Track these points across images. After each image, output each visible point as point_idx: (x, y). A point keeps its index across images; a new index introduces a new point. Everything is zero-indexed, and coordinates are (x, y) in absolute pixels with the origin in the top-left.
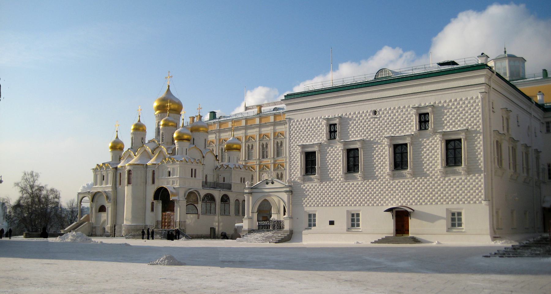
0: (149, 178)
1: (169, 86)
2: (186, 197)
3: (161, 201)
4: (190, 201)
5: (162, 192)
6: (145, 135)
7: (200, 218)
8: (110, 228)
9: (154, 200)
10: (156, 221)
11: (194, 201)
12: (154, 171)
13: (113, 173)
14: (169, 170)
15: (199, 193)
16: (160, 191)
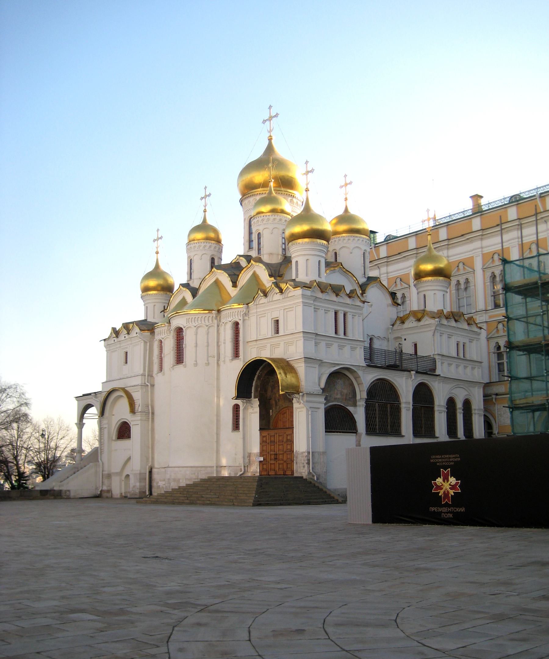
0: (225, 343)
1: (270, 140)
2: (323, 385)
3: (256, 402)
4: (335, 399)
5: (259, 378)
6: (220, 251)
7: (361, 443)
8: (138, 477)
9: (238, 397)
10: (247, 455)
11: (346, 399)
12: (237, 324)
13: (145, 343)
14: (275, 315)
15: (357, 378)
16: (256, 374)
